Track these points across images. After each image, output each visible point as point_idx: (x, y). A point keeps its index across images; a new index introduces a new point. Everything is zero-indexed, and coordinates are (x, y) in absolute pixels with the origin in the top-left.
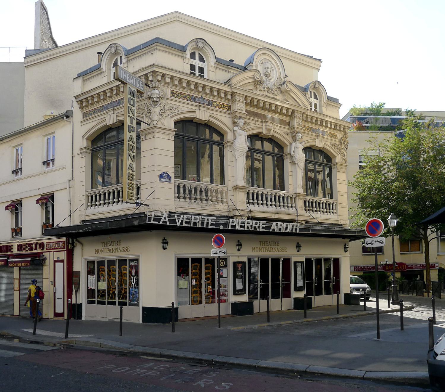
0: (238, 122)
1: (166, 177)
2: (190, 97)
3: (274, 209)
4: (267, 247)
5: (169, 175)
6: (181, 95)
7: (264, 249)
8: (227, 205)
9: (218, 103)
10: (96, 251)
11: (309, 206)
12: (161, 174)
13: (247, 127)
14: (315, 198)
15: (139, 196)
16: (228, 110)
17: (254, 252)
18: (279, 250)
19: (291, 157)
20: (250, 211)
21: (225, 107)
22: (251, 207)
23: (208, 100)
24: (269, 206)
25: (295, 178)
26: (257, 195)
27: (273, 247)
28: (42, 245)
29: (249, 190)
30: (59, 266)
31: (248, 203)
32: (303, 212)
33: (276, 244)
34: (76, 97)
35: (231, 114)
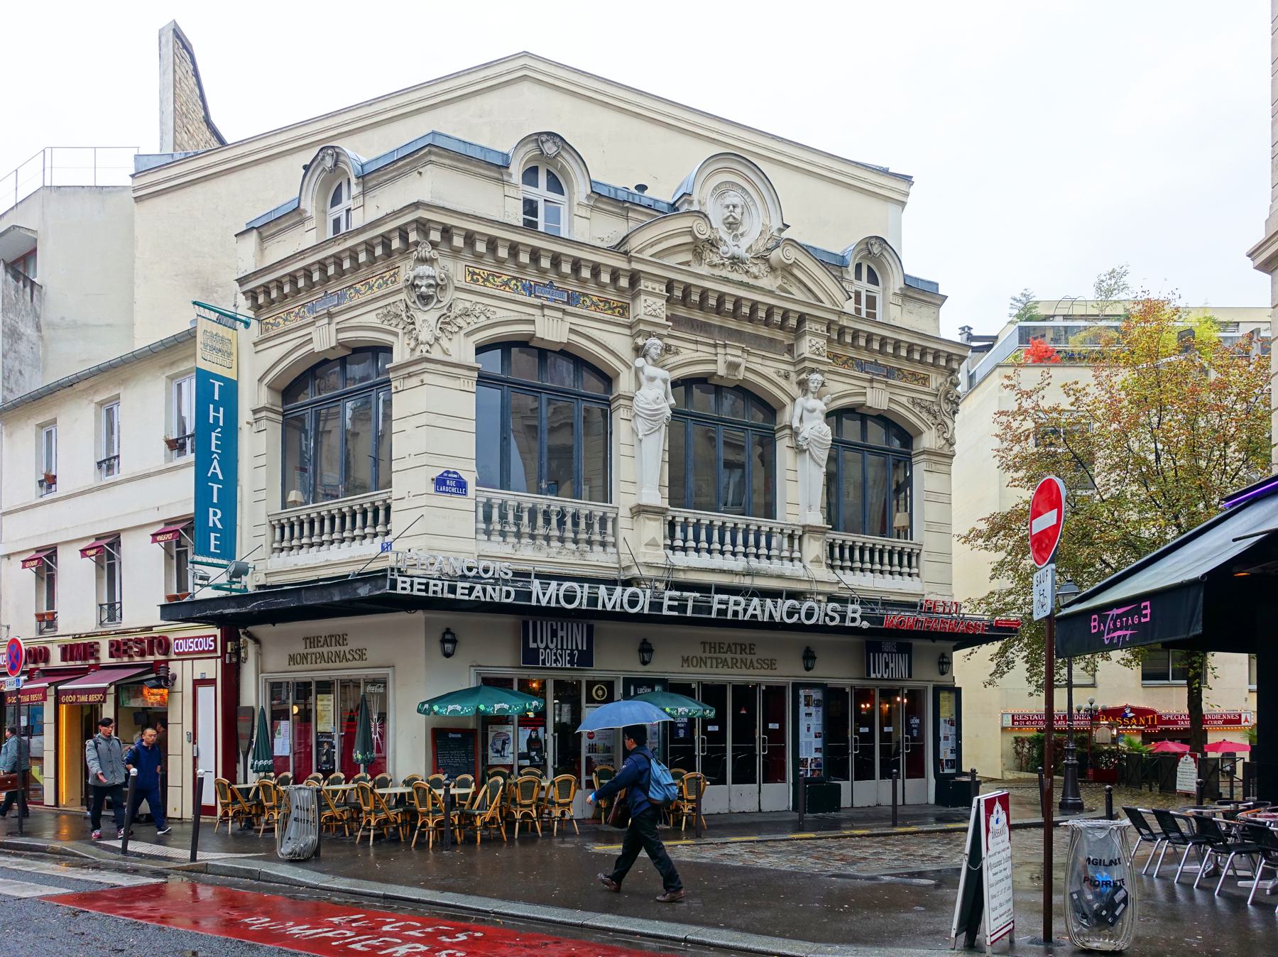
3: (739, 564)
4: (723, 656)
8: (614, 550)
9: (595, 299)
10: (292, 659)
11: (837, 556)
13: (672, 360)
16: (622, 315)
17: (686, 669)
18: (756, 665)
20: (672, 569)
22: (679, 559)
23: (566, 291)
24: (728, 556)
25: (800, 490)
27: (738, 656)
28: (163, 644)
29: (674, 518)
30: (206, 694)
31: (673, 548)
32: (822, 573)
34: (241, 281)
35: (630, 327)
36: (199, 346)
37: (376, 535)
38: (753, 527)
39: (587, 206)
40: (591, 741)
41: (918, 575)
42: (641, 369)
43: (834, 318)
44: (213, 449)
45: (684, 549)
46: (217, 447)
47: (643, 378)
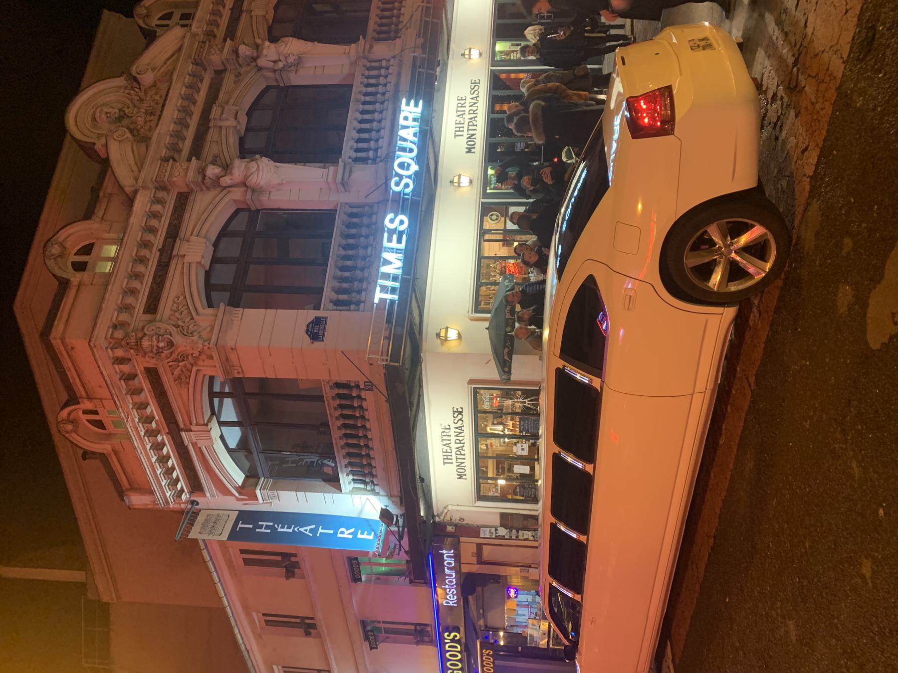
1: (317, 327)
5: (312, 322)
7: (471, 128)
12: (309, 336)
15: (353, 384)
18: (475, 95)
26: (359, 141)
33: (462, 102)
36: (211, 537)
37: (359, 397)
44: (291, 531)
46: (289, 528)
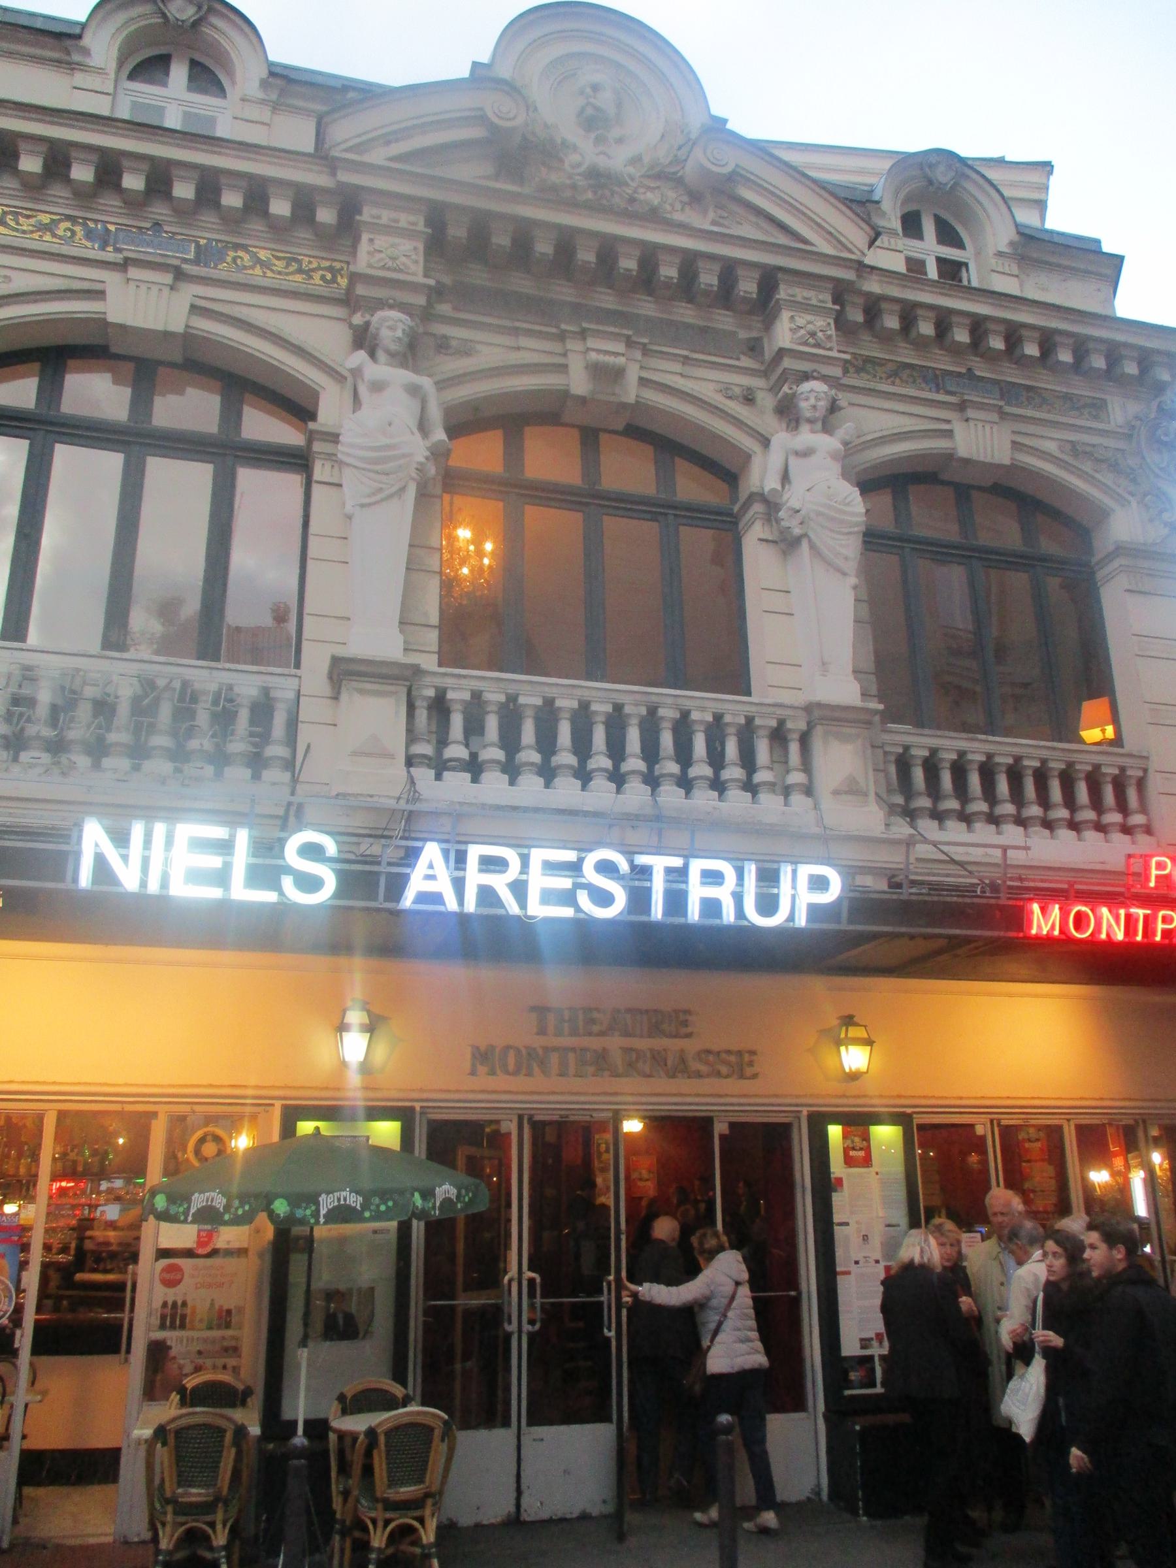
0: (372, 329)
2: (78, 229)
6: (21, 220)
14: (976, 745)
19: (771, 506)
21: (313, 270)
38: (668, 713)
39: (263, 102)
40: (172, 1294)
41: (1148, 830)
42: (357, 372)
43: (848, 275)
45: (474, 768)
47: (363, 390)
